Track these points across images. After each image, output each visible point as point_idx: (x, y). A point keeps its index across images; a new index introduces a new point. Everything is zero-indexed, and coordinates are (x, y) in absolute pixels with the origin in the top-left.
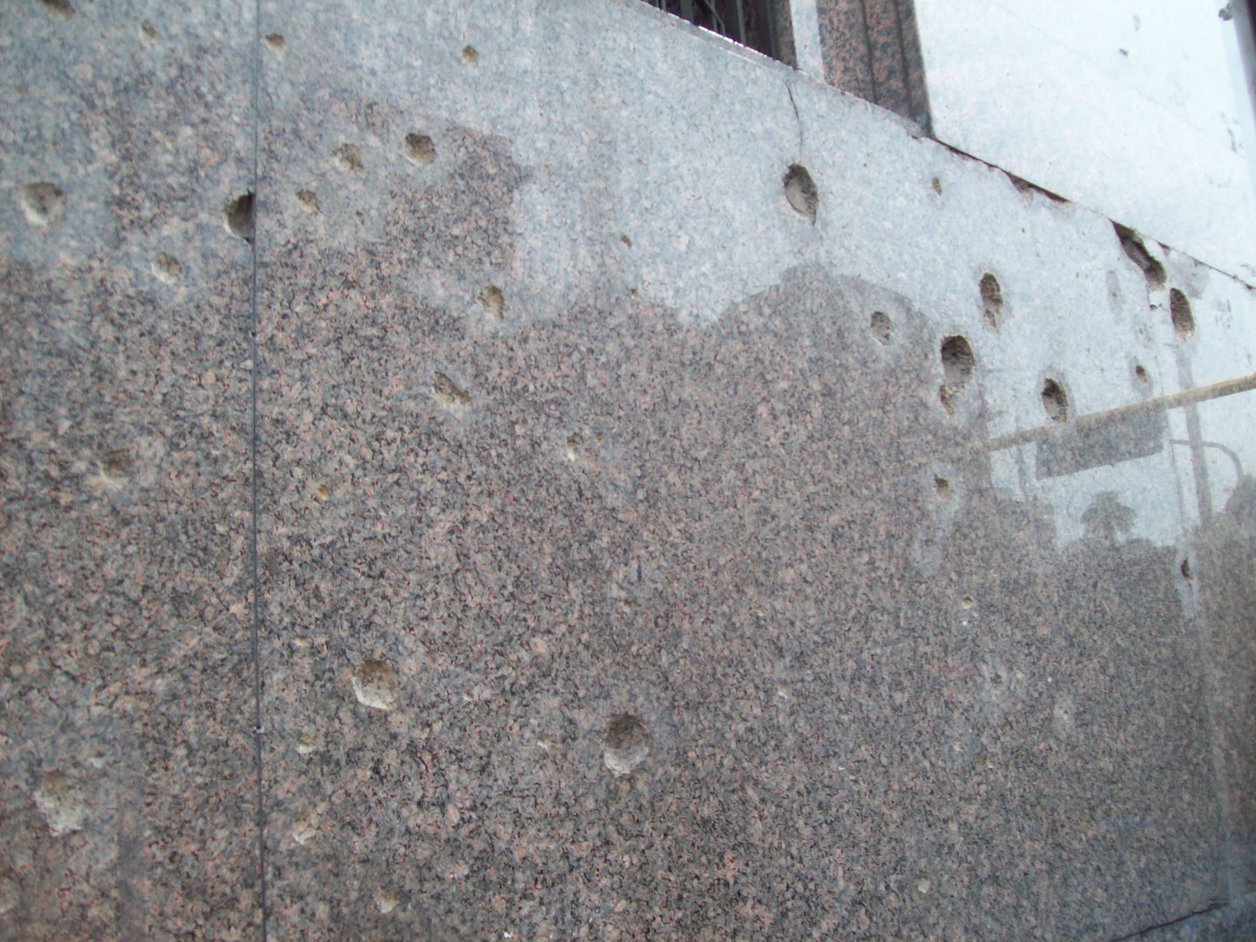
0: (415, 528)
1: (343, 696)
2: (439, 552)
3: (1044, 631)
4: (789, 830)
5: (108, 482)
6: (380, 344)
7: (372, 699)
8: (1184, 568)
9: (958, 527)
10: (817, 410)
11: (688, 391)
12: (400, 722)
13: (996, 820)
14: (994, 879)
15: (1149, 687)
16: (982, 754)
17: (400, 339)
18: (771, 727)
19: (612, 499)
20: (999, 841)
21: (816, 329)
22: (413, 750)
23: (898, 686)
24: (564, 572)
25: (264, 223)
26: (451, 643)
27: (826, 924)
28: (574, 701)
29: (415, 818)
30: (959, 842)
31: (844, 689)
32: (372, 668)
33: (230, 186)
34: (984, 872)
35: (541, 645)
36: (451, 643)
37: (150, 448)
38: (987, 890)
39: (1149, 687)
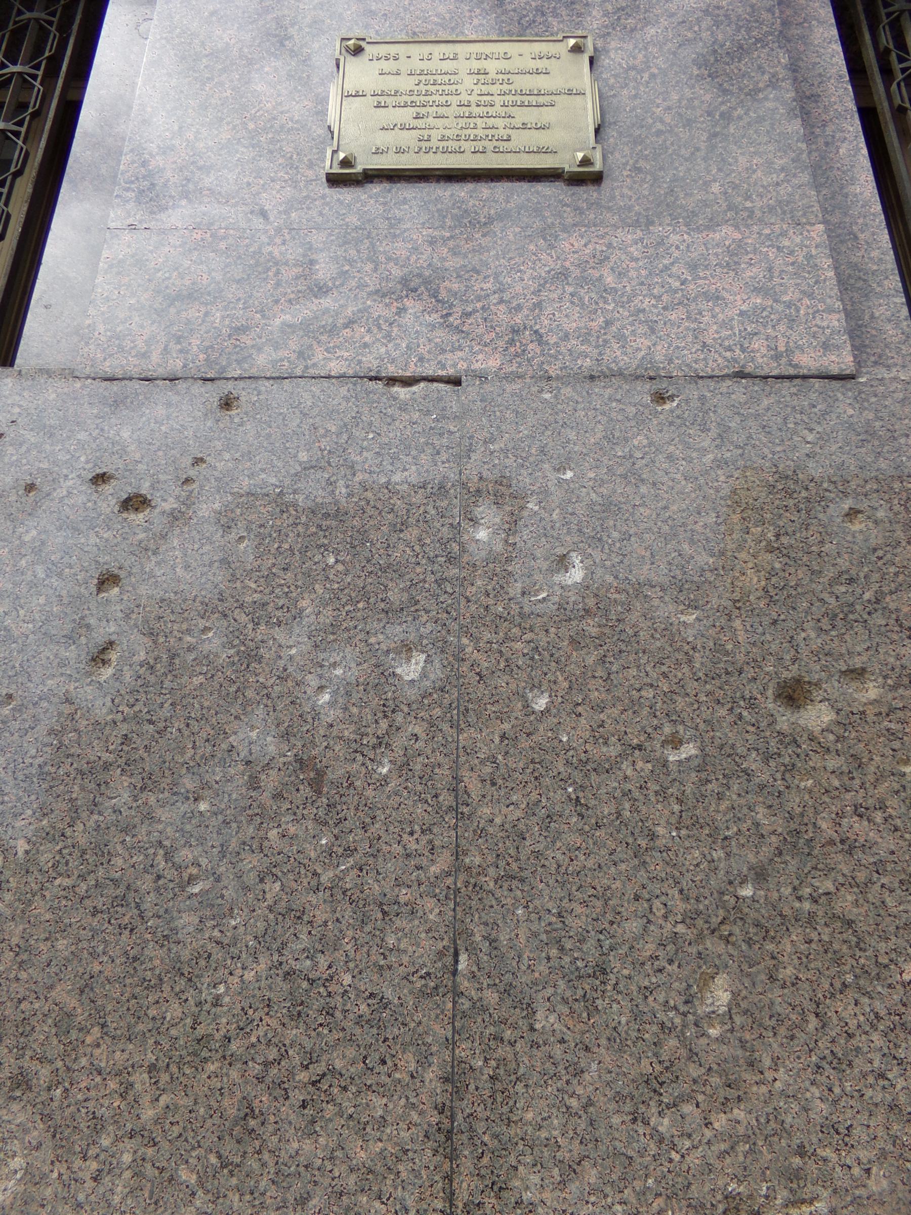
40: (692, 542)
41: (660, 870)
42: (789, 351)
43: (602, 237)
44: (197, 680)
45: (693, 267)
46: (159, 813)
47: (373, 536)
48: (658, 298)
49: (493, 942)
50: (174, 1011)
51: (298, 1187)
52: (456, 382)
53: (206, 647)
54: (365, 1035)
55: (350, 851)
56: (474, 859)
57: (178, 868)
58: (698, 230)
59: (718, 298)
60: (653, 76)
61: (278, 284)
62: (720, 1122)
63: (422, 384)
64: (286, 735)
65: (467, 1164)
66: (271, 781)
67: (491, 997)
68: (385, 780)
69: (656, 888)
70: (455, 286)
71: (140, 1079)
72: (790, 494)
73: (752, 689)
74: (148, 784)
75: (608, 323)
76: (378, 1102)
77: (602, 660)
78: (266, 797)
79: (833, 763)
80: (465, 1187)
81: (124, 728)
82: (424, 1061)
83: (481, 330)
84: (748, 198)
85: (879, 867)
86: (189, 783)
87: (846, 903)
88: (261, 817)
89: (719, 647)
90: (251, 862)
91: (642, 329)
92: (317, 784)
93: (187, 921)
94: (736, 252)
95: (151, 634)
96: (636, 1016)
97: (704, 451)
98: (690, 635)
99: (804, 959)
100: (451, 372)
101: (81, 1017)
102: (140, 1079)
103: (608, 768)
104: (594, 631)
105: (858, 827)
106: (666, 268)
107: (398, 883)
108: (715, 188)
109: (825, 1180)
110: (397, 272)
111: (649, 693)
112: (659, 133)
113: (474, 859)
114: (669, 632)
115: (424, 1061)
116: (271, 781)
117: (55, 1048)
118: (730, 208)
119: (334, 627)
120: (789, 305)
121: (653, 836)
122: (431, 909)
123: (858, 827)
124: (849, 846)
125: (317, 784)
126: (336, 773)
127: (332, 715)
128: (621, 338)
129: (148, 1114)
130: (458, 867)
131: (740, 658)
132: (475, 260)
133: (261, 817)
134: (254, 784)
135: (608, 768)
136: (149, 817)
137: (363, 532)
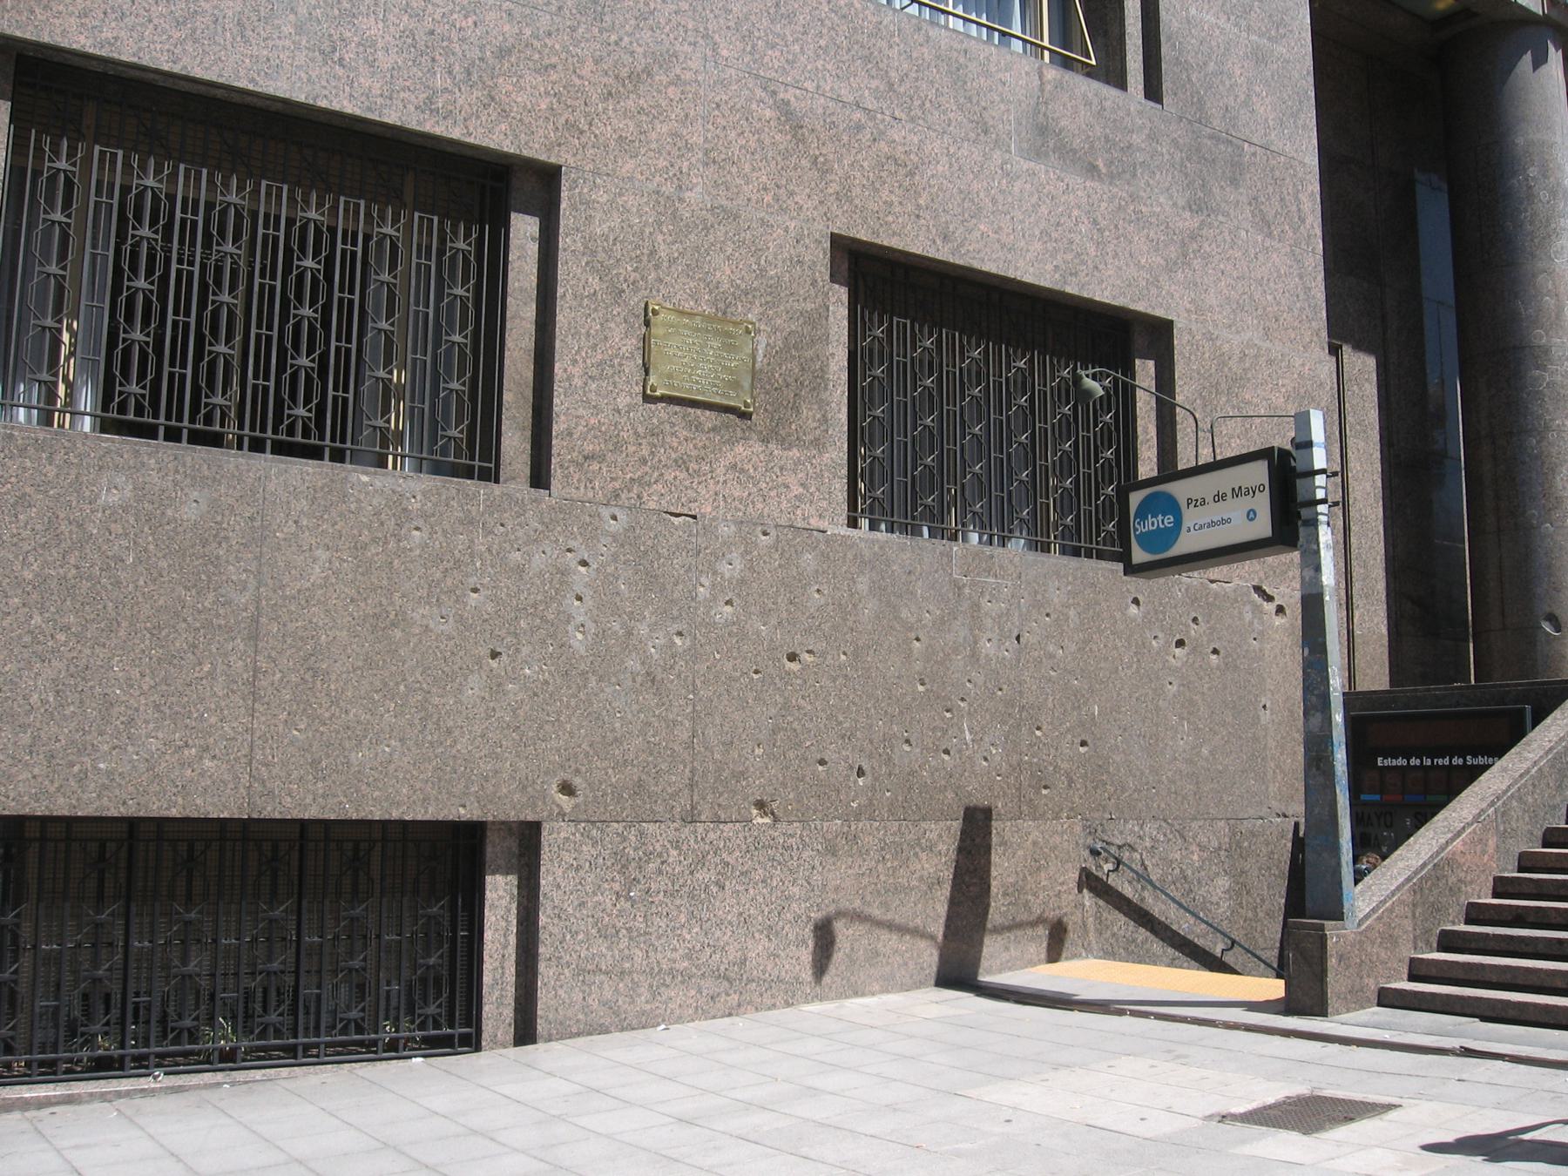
0: (1046, 699)
1: (1034, 733)
2: (1050, 705)
3: (1202, 726)
4: (1119, 771)
5: (1000, 693)
6: (1041, 662)
7: (1038, 733)
8: (1264, 707)
9: (1174, 695)
10: (1135, 666)
11: (1102, 665)
12: (1043, 738)
13: (1178, 777)
14: (1176, 793)
15: (1241, 746)
16: (1175, 759)
17: (1044, 660)
18: (1116, 746)
19: (1084, 692)
20: (1178, 783)
21: (1137, 643)
22: (1044, 744)
23: (1151, 738)
24: (1073, 708)
25: (1021, 639)
26: (1052, 723)
27: (1127, 794)
28: (1074, 736)
29: (1044, 757)
30: (1166, 782)
31: (1136, 738)
32: (1039, 728)
33: (1015, 634)
34: (1173, 790)
35: (1068, 724)
36: (1052, 723)
37: (1005, 687)
38: (1173, 796)
39: (1241, 746)
40: (768, 599)
41: (748, 713)
42: (808, 517)
43: (750, 447)
44: (613, 641)
45: (781, 469)
46: (606, 689)
47: (667, 587)
48: (768, 484)
49: (703, 734)
50: (617, 752)
51: (654, 799)
52: (694, 517)
53: (614, 629)
54: (669, 760)
55: (663, 705)
56: (698, 708)
57: (614, 709)
58: (785, 449)
59: (788, 487)
60: (777, 352)
61: (627, 455)
62: (757, 782)
63: (683, 517)
64: (643, 663)
65: (696, 793)
66: (639, 679)
67: (702, 749)
68: (673, 681)
69: (747, 719)
70: (696, 467)
71: (610, 771)
72: (800, 581)
73: (780, 656)
74: (601, 679)
75: (750, 494)
76: (674, 778)
77: (737, 642)
78: (638, 686)
79: (799, 681)
80: (696, 798)
81: (591, 658)
82: (685, 767)
83: (704, 492)
84: (805, 434)
85: (805, 715)
86: (613, 680)
87: (795, 725)
88: (638, 693)
89: (772, 640)
90: (635, 707)
91: (761, 499)
92: (653, 681)
93: (618, 725)
94: (797, 463)
95: (595, 622)
96: (739, 755)
97: (776, 560)
98: (763, 634)
99: (782, 740)
100: (693, 513)
101: (591, 753)
102: (610, 771)
103: (736, 680)
104: (735, 631)
105: (801, 701)
106: (772, 468)
107: (678, 715)
108: (793, 427)
109: (780, 795)
110: (674, 456)
111: (750, 655)
112: (776, 389)
113: (698, 708)
114: (758, 633)
115: (685, 767)
116: (639, 679)
117: (585, 762)
118: (798, 439)
119: (656, 623)
120: (811, 494)
121: (748, 703)
122: (687, 723)
123: (801, 701)
124: (799, 708)
125: (653, 681)
126: (659, 678)
127: (656, 657)
128: (753, 502)
129: (614, 780)
130: (694, 710)
131: (777, 643)
132: (703, 453)
133: (638, 693)
134: (634, 681)
135: (736, 680)
136: (603, 691)
137: (663, 584)
